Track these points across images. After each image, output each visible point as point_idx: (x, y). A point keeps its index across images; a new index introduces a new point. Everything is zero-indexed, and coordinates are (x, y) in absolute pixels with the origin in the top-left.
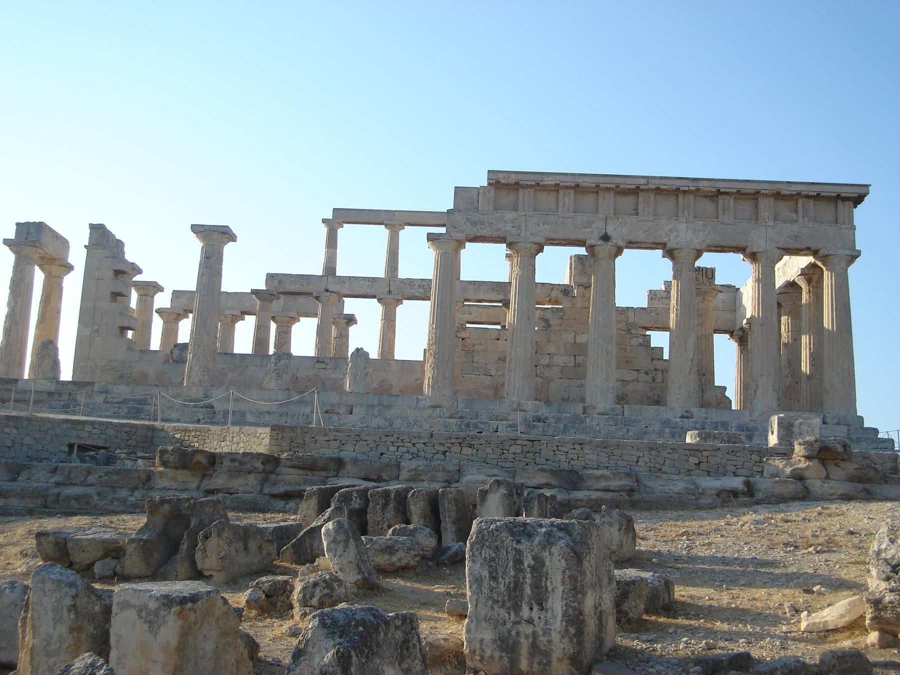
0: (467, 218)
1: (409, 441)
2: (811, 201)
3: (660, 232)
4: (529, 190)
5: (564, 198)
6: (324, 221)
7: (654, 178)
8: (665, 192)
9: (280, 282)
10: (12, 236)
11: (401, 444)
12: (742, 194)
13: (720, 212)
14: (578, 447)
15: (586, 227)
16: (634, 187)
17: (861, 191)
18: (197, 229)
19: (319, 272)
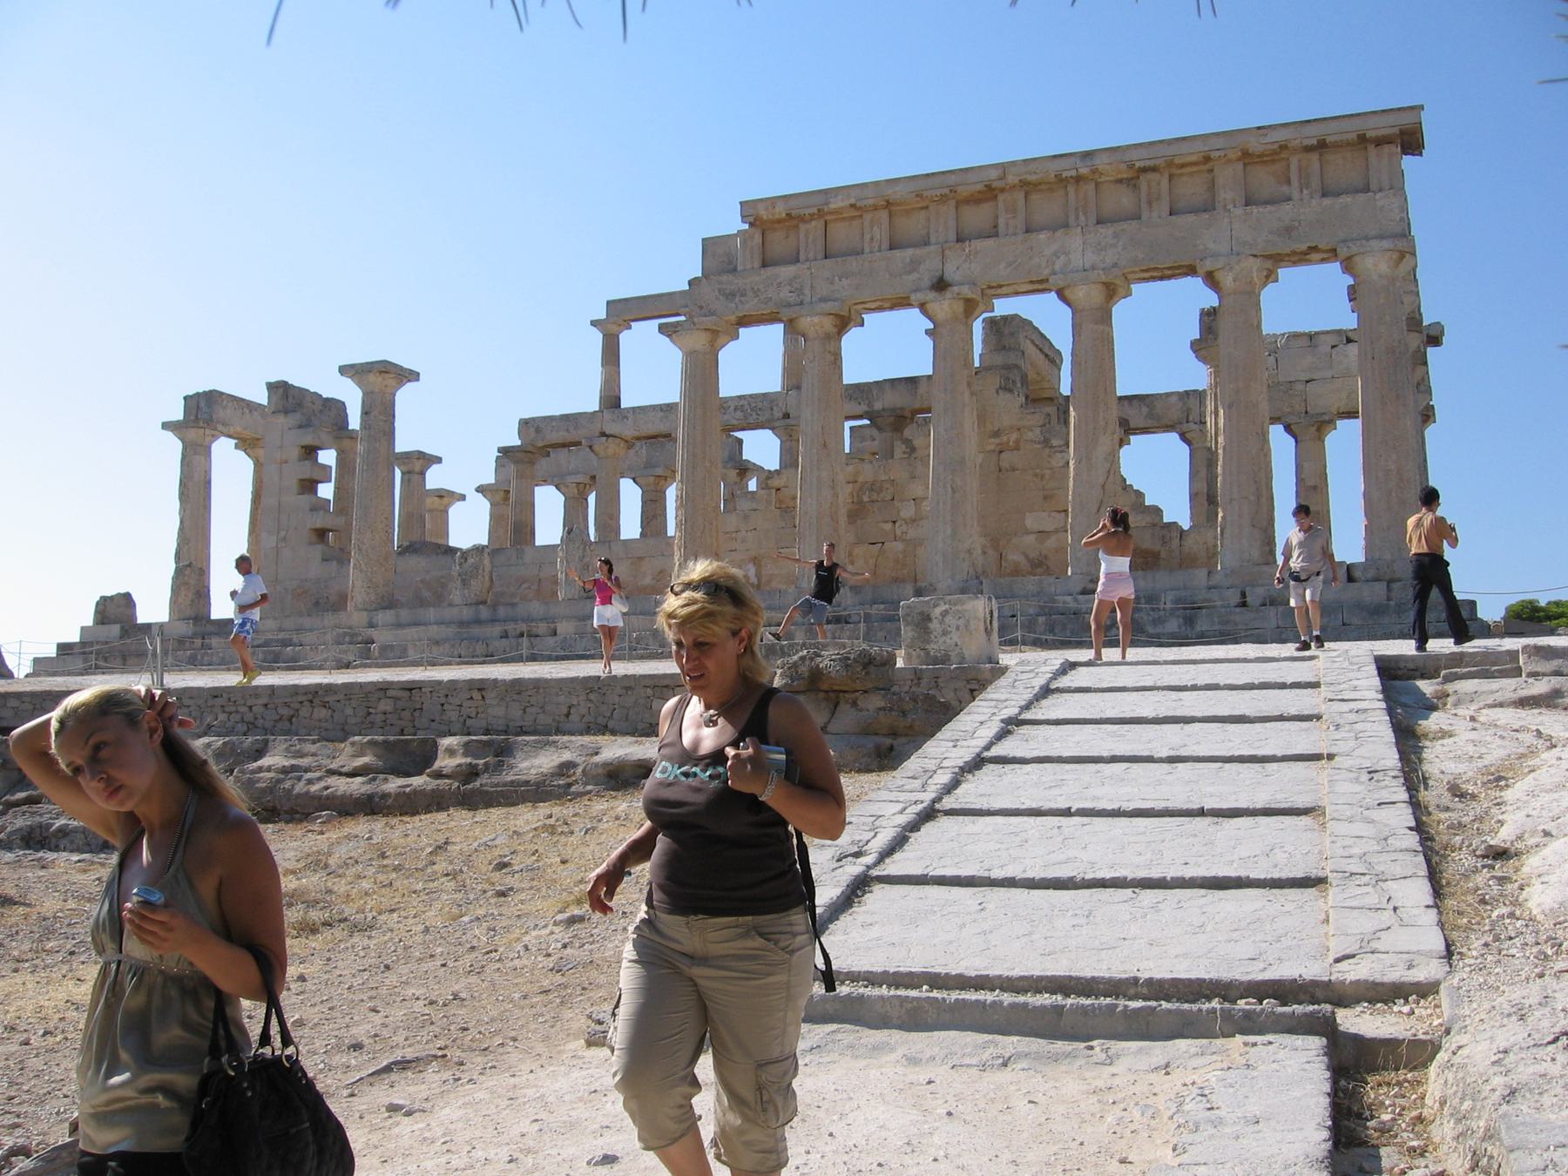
0: (719, 290)
1: (243, 702)
2: (1314, 157)
3: (1036, 260)
4: (814, 223)
5: (872, 228)
6: (594, 323)
7: (1013, 163)
8: (1043, 187)
9: (538, 430)
10: (178, 414)
11: (233, 709)
12: (1183, 166)
13: (1144, 205)
14: (477, 695)
15: (910, 273)
16: (980, 187)
17: (1406, 120)
18: (344, 370)
19: (594, 406)
